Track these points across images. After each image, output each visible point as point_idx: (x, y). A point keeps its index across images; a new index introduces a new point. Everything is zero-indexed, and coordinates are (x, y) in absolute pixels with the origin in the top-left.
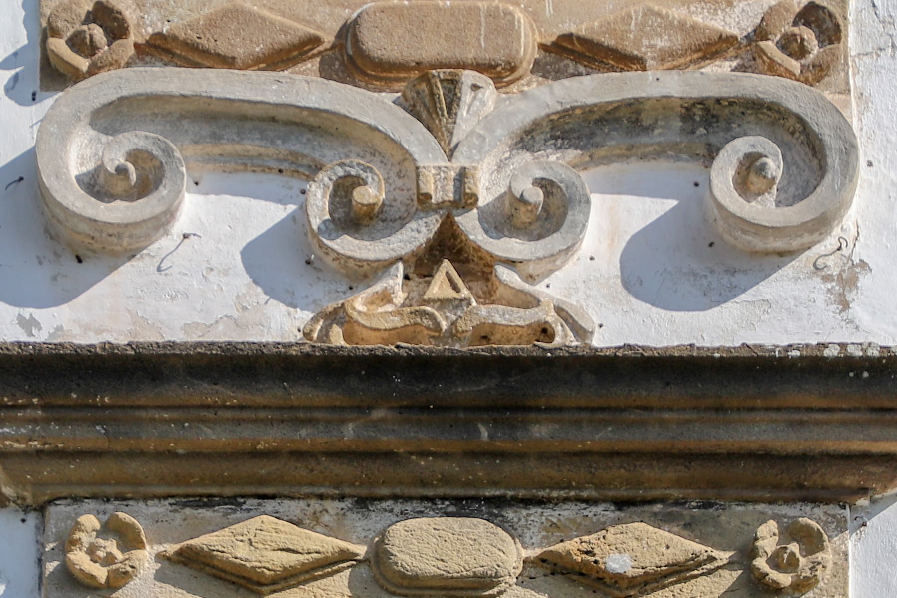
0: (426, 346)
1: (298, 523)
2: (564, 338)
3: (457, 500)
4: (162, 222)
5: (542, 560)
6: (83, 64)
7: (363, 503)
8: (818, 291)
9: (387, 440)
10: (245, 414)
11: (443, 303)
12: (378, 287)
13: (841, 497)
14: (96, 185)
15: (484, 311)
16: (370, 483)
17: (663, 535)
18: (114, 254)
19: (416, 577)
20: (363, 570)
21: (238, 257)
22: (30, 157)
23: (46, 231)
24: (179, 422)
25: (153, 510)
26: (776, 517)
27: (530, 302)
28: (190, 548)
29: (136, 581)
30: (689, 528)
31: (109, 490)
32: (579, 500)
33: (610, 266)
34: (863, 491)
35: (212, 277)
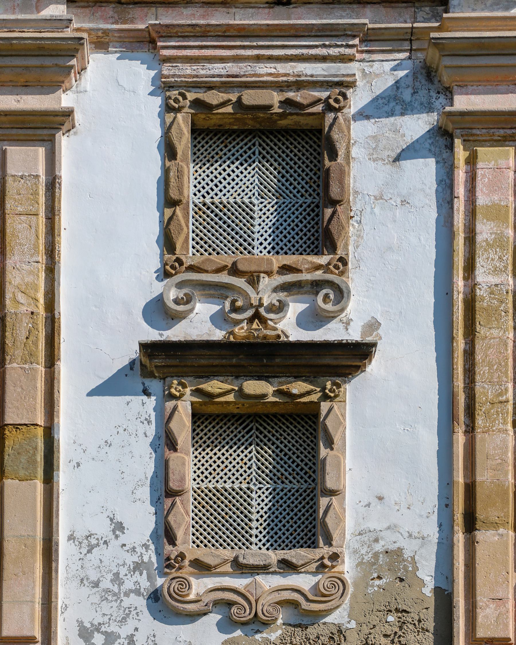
0: (252, 341)
1: (222, 382)
2: (283, 338)
3: (258, 376)
4: (191, 310)
5: (277, 390)
6: (173, 272)
7: (237, 377)
8: (341, 326)
9: (243, 363)
11: (256, 330)
12: (241, 326)
14: (177, 301)
15: (265, 331)
16: (239, 373)
18: (181, 318)
19: (249, 395)
20: (237, 393)
22: (161, 295)
24: (196, 359)
27: (275, 329)
30: (311, 383)
32: (286, 376)
33: (294, 320)
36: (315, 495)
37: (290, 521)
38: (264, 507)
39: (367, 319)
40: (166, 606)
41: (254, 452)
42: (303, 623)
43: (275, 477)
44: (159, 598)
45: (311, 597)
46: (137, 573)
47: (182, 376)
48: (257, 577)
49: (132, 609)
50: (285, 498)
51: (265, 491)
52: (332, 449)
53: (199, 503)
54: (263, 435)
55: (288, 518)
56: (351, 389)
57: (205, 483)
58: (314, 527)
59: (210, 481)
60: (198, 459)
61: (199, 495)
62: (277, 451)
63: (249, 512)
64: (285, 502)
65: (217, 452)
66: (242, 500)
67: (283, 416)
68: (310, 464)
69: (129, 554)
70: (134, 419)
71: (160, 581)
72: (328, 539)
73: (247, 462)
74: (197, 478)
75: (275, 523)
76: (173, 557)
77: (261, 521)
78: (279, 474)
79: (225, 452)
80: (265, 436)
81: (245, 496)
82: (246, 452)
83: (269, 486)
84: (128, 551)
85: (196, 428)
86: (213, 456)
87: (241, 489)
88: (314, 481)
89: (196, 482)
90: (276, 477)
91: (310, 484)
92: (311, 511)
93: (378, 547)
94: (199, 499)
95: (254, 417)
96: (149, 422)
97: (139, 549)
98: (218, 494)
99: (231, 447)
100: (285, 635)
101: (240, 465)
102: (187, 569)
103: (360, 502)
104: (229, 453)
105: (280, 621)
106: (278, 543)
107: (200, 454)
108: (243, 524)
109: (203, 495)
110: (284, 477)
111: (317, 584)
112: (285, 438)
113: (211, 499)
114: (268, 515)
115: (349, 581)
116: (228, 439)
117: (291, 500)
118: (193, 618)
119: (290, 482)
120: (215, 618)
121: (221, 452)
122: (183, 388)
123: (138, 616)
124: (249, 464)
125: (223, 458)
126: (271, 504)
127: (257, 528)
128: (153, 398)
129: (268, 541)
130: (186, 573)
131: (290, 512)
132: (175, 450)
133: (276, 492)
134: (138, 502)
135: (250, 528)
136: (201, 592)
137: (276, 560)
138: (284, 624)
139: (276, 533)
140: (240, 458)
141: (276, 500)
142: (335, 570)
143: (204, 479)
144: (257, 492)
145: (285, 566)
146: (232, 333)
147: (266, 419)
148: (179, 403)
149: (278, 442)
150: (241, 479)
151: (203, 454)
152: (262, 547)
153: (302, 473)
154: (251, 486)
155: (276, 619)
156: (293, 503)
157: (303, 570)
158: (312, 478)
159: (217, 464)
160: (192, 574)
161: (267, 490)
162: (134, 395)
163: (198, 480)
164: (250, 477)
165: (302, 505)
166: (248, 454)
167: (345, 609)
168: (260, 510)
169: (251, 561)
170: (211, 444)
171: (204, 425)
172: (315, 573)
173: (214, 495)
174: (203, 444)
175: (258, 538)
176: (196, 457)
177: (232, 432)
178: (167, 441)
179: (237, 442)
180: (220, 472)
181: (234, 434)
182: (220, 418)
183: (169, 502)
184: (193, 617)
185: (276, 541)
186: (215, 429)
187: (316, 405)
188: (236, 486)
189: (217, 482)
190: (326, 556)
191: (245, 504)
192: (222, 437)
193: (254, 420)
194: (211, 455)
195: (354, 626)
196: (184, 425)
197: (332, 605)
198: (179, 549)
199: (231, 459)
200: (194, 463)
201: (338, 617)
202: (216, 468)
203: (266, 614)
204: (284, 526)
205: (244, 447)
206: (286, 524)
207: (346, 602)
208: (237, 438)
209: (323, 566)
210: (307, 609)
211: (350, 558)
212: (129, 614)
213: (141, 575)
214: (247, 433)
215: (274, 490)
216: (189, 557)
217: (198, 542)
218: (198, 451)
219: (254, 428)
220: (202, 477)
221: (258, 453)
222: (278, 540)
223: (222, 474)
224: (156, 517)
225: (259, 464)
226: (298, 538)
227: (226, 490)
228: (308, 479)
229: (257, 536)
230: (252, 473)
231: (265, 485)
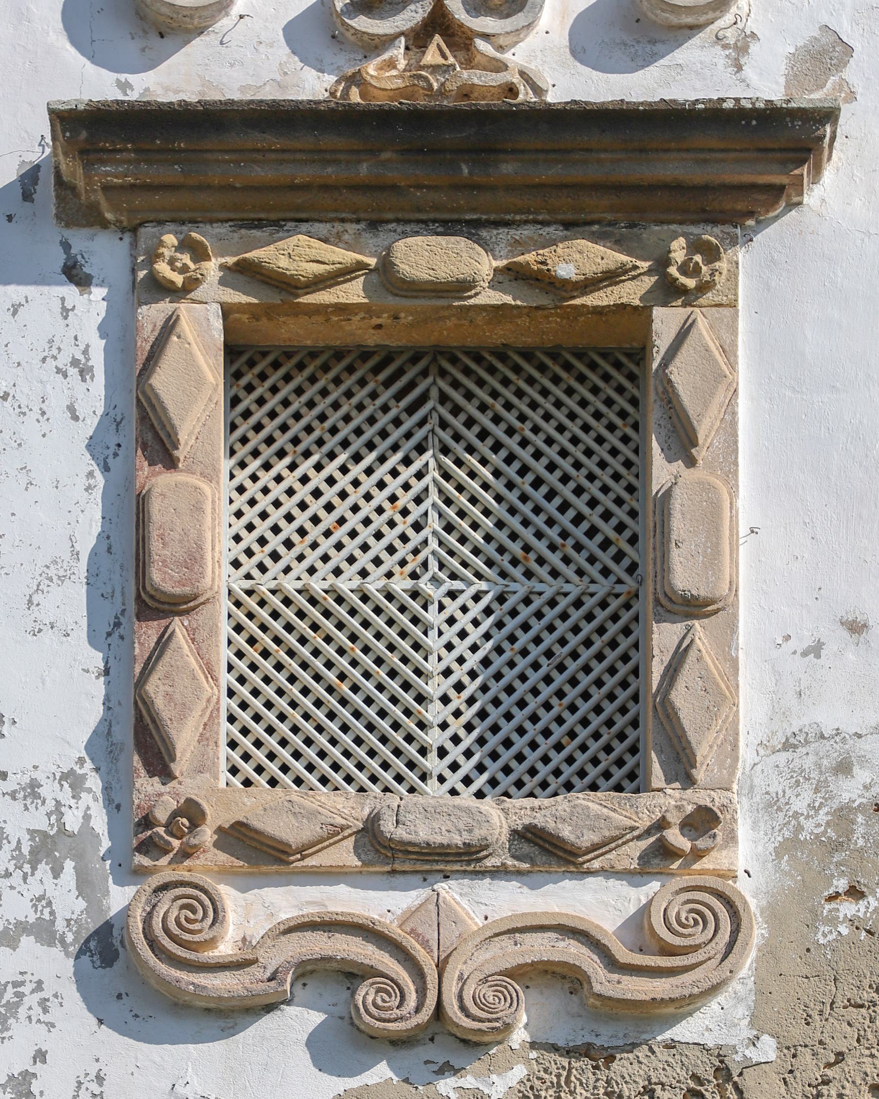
0: (422, 102)
1: (325, 241)
2: (525, 95)
3: (444, 222)
5: (508, 269)
7: (374, 225)
8: (719, 57)
9: (392, 175)
10: (286, 156)
11: (435, 69)
12: (386, 56)
13: (734, 218)
15: (465, 74)
16: (380, 210)
17: (599, 249)
19: (413, 282)
20: (374, 277)
21: (281, 33)
23: (137, 13)
24: (237, 162)
25: (217, 230)
26: (685, 235)
27: (500, 67)
28: (245, 260)
29: (205, 285)
30: (619, 244)
31: (184, 216)
32: (536, 222)
33: (561, 39)
34: (751, 214)
35: (262, 48)
36: (636, 619)
37: (554, 701)
38: (468, 654)
39: (805, 32)
40: (139, 979)
41: (434, 473)
42: (598, 1042)
43: (502, 559)
44: (115, 956)
45: (624, 955)
46: (44, 868)
47: (194, 221)
48: (442, 887)
49: (26, 989)
50: (537, 626)
51: (470, 604)
52: (691, 462)
53: (252, 641)
54: (463, 417)
55: (546, 691)
56: (752, 264)
57: (269, 575)
58: (635, 724)
59: (287, 570)
60: (247, 496)
61: (250, 616)
62: (511, 471)
63: (418, 672)
64: (537, 640)
65: (312, 473)
66: (392, 633)
67: (527, 355)
68: (621, 514)
69: (18, 806)
70: (37, 362)
71: (119, 897)
72: (678, 760)
73: (411, 506)
74: (243, 558)
75: (502, 709)
76: (162, 815)
77: (458, 701)
78: (515, 548)
79: (337, 475)
80: (470, 423)
81: (404, 620)
82: (407, 473)
83: (483, 586)
84: (13, 795)
85: (242, 394)
86: (297, 486)
87: (390, 597)
88: (632, 569)
89: (243, 571)
90: (507, 557)
91: (619, 581)
92: (623, 670)
93: (850, 790)
94: (252, 627)
95: (434, 360)
96: (85, 372)
97: (49, 790)
98: (315, 613)
99: (357, 458)
100: (537, 1083)
101: (385, 516)
102: (211, 857)
103: (788, 638)
104: (350, 477)
105: (519, 1036)
106: (513, 777)
107: (254, 478)
108: (396, 712)
109: (264, 614)
110: (532, 556)
111: (645, 910)
112: (536, 430)
113: (289, 628)
114: (479, 681)
115: (753, 903)
116: (345, 431)
117: (556, 634)
118: (230, 1022)
119: (555, 573)
120: (301, 1020)
121: (325, 473)
122: (195, 260)
123: (45, 1010)
124: (416, 512)
125: (330, 494)
126: (489, 645)
127: (444, 726)
128: (98, 293)
129: (481, 768)
130: (207, 871)
131: (555, 674)
132: (171, 463)
133: (507, 606)
134: (48, 636)
135: (422, 725)
136: (257, 929)
137: (505, 831)
138: (533, 1045)
139: (507, 743)
140: (387, 492)
141: (505, 631)
142: (705, 863)
143: (268, 562)
144: (441, 608)
145: (535, 850)
146: (355, 79)
147: (473, 366)
148: (184, 308)
149: (512, 443)
150: (390, 562)
151: (266, 478)
152: (460, 787)
153: (592, 545)
154: (424, 585)
155: (508, 1028)
156: (563, 642)
157: (596, 864)
158: (626, 562)
159: (309, 513)
160: (225, 874)
161: (477, 598)
162: (36, 283)
163: (249, 565)
164: (421, 557)
165: (594, 649)
166: (413, 481)
167: (738, 999)
168: (455, 666)
169: (423, 832)
170: (289, 447)
171: (268, 383)
172: (637, 875)
173: (301, 614)
174: (262, 447)
175: (448, 760)
176: (241, 489)
177: (360, 407)
178: (143, 433)
179: (377, 440)
180: (321, 540)
181: (366, 413)
182: (318, 362)
183: (148, 634)
184: (229, 1016)
185: (507, 770)
186: (304, 398)
187: (638, 317)
188: (374, 585)
189: (312, 571)
190: (675, 818)
191: (405, 646)
192: (328, 424)
193: (433, 370)
194: (290, 482)
195: (772, 1056)
196: (200, 381)
197: (694, 984)
198: (181, 789)
199: (355, 496)
200: (235, 507)
201: (717, 1023)
202: (308, 526)
203: (474, 1010)
204: (534, 718)
205: (399, 455)
206: (541, 712)
207: (744, 972)
208: (378, 426)
209: (664, 852)
210: (611, 993)
211: (755, 826)
212: (18, 1005)
213: (56, 876)
214: (411, 410)
215: (501, 599)
216: (216, 817)
217: (248, 769)
218: (249, 471)
219: (434, 393)
220: (261, 555)
221: (447, 476)
222: (514, 764)
223: (326, 545)
224: (108, 684)
225: (451, 512)
226: (581, 758)
227: (340, 600)
228: (612, 565)
229: (442, 753)
230: (425, 542)
231: (470, 584)
